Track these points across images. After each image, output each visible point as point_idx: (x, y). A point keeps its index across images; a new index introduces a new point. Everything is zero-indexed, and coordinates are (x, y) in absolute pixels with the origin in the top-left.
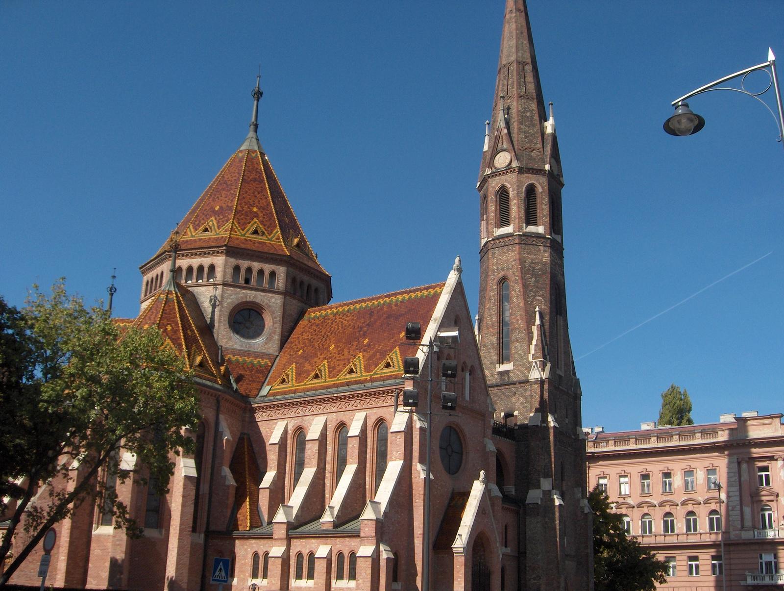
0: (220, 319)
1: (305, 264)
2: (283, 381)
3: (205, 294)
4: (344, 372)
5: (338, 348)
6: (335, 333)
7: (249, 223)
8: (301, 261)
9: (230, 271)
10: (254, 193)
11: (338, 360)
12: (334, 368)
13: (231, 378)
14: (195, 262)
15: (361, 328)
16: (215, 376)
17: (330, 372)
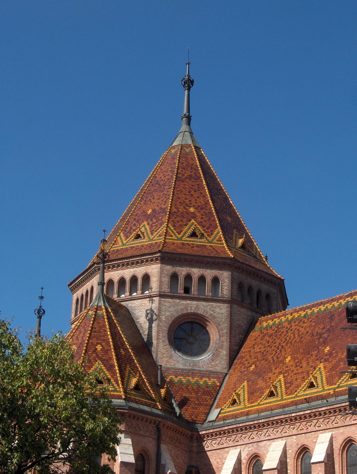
0: (158, 335)
1: (253, 268)
2: (234, 402)
3: (140, 308)
4: (303, 388)
5: (295, 360)
6: (291, 343)
7: (186, 225)
8: (247, 263)
9: (166, 280)
10: (189, 192)
11: (296, 374)
12: (291, 383)
13: (173, 401)
14: (127, 273)
15: (321, 335)
16: (154, 401)
17: (287, 388)
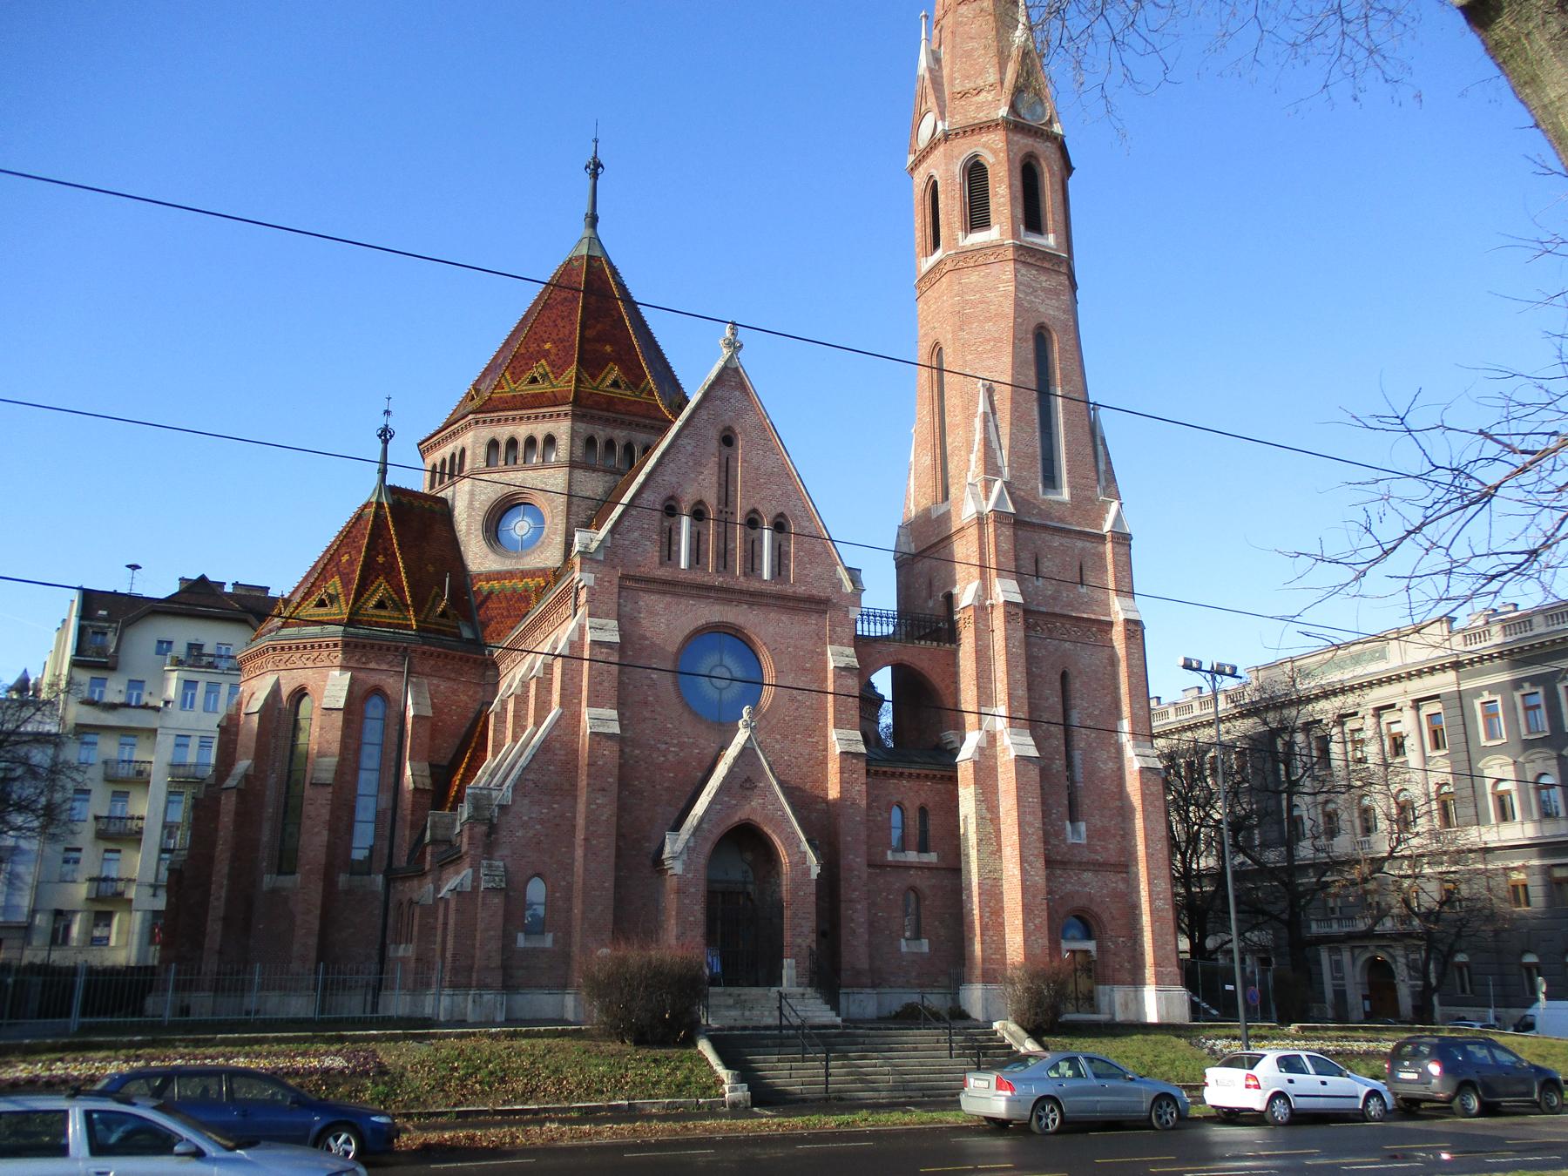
9: (482, 451)
